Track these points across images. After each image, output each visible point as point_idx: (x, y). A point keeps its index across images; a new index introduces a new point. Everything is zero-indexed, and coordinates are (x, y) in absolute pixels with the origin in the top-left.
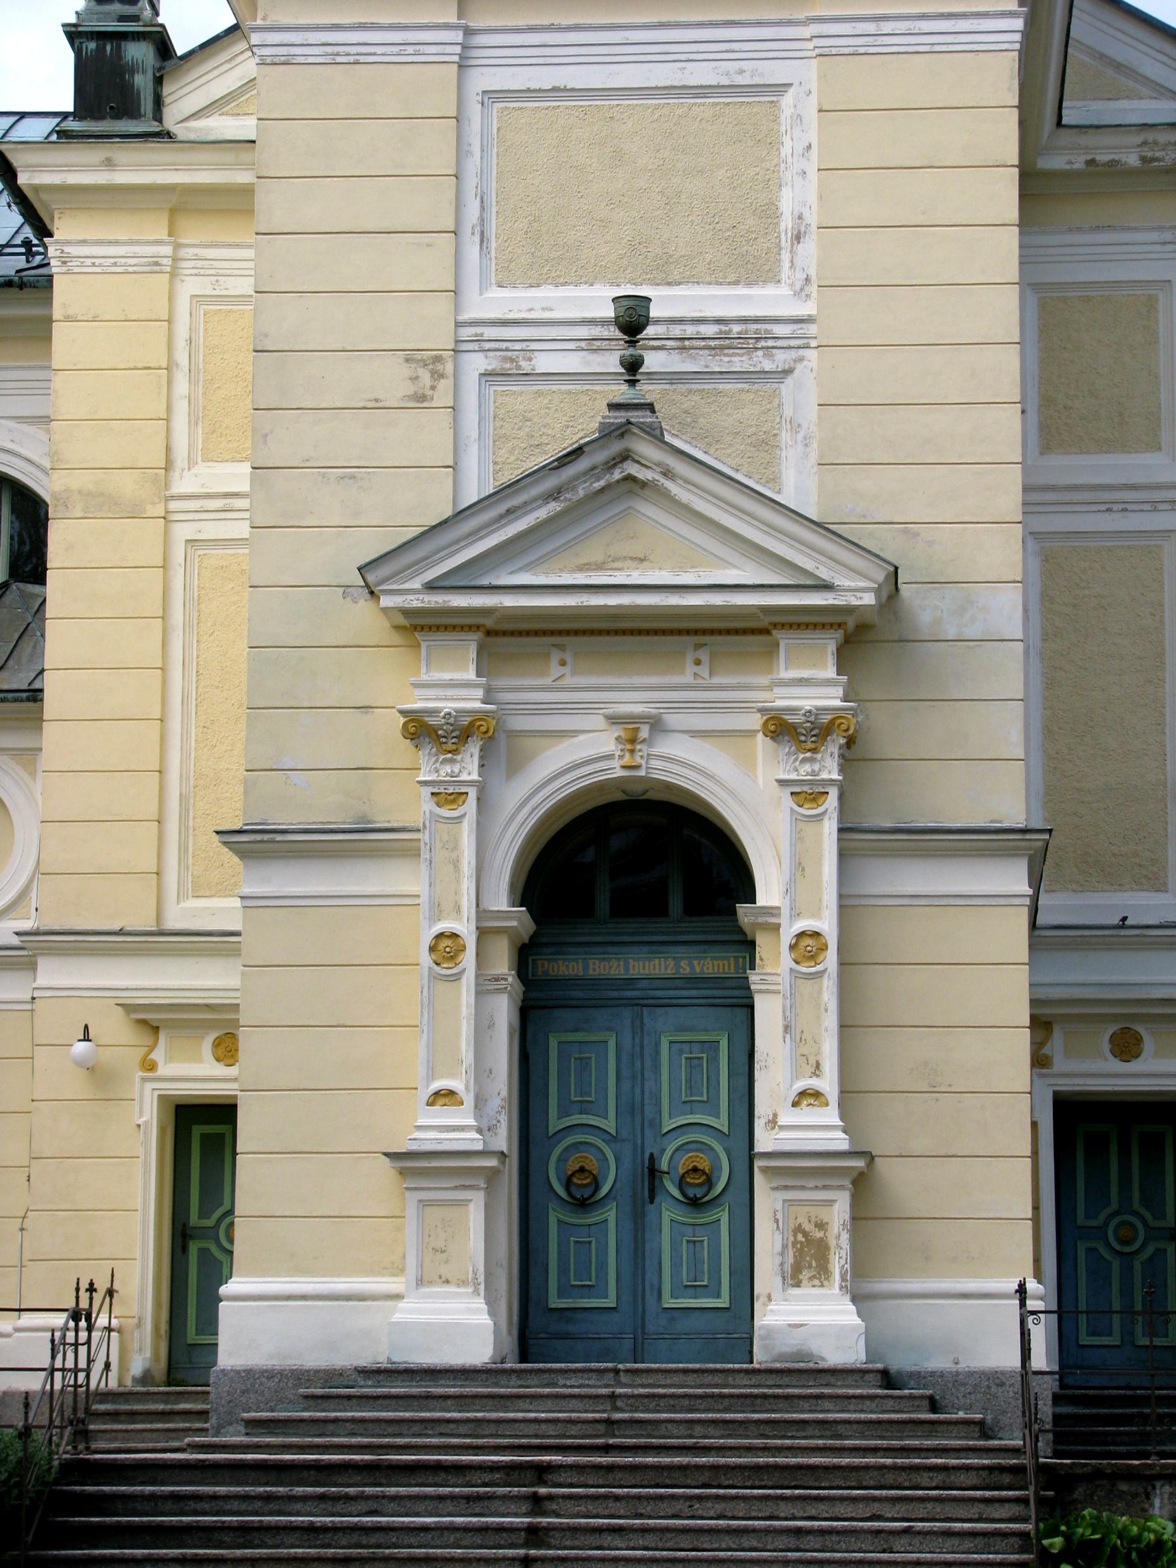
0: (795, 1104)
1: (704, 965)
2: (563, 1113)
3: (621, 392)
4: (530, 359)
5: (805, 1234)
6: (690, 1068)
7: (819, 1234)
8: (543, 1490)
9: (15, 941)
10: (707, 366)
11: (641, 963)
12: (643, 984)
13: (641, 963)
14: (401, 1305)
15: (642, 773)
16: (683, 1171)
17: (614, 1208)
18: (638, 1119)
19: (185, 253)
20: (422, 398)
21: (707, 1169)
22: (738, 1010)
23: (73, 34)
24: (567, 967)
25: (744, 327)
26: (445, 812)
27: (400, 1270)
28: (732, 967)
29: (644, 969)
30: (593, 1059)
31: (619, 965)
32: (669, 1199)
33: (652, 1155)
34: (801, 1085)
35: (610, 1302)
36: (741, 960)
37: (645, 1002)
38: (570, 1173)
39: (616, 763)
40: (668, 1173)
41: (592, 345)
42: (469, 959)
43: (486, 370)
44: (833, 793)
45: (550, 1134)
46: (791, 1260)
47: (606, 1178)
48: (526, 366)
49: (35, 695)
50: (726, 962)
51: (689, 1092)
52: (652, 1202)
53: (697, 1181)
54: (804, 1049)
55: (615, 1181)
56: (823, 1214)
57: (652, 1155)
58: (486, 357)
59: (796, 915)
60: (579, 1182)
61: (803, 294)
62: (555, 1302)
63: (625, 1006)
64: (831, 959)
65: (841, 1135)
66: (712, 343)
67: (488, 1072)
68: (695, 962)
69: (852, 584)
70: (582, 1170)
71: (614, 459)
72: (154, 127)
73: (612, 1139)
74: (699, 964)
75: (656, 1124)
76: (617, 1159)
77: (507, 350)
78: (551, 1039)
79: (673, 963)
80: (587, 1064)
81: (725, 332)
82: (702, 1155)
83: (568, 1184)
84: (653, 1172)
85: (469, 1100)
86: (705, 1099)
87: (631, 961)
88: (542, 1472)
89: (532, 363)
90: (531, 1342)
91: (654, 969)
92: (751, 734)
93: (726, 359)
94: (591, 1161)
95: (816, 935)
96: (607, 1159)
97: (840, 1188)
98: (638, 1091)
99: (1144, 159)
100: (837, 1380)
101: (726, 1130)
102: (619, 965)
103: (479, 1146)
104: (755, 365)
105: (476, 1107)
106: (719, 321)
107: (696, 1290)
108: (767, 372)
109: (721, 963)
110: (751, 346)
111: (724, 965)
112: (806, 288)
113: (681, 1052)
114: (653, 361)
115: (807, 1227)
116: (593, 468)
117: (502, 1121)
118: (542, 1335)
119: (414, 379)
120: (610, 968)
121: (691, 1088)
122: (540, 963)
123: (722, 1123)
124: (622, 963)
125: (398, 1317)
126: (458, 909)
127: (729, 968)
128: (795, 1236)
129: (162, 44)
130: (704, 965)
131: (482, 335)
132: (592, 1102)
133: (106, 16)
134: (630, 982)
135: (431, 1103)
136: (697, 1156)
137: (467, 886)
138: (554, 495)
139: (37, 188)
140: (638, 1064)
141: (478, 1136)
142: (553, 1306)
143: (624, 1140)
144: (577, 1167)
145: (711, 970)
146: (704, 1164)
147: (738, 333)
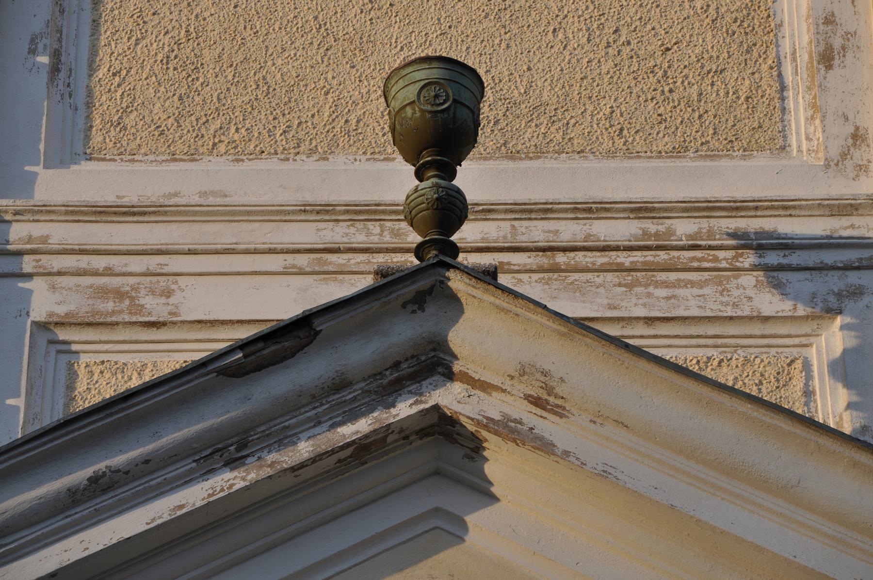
4: (168, 293)
10: (613, 307)
25: (704, 224)
43: (51, 315)
58: (53, 288)
61: (849, 164)
71: (396, 365)
77: (109, 272)
81: (657, 235)
89: (172, 300)
93: (662, 292)
108: (766, 319)
110: (724, 265)
112: (856, 154)
116: (340, 384)
131: (45, 239)
147: (690, 237)
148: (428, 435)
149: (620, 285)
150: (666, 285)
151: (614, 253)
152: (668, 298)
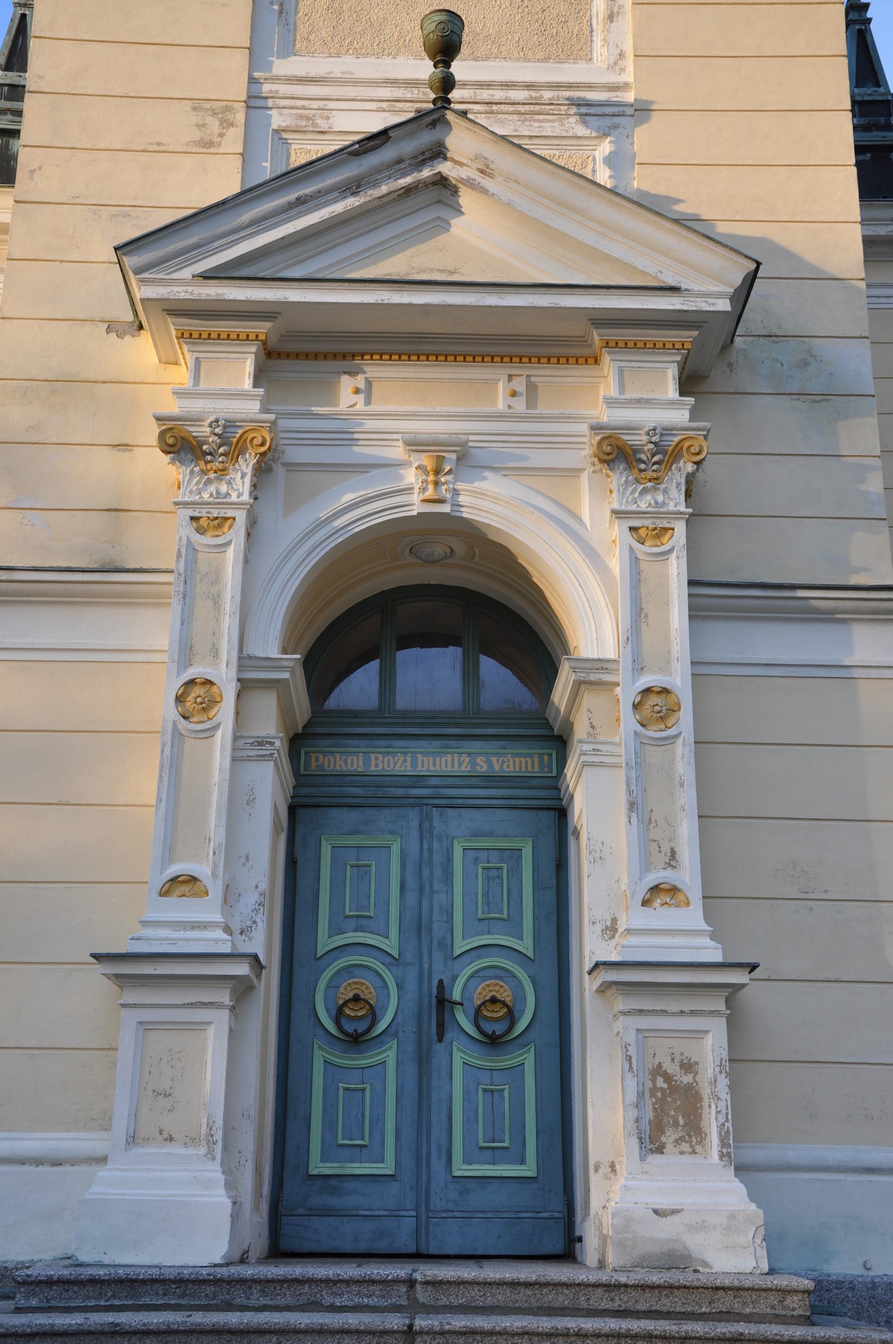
0: (645, 903)
1: (503, 762)
2: (336, 930)
4: (328, 118)
5: (668, 1078)
6: (488, 879)
7: (687, 1079)
10: (516, 131)
11: (431, 759)
12: (433, 781)
13: (431, 759)
14: (103, 1173)
15: (446, 508)
16: (479, 1003)
17: (395, 1046)
18: (425, 939)
20: (210, 144)
21: (508, 1000)
22: (543, 814)
24: (345, 762)
25: (556, 93)
26: (207, 540)
27: (105, 1123)
28: (536, 765)
29: (434, 765)
30: (373, 866)
31: (405, 761)
32: (463, 1038)
33: (441, 982)
34: (654, 878)
35: (387, 1168)
36: (546, 758)
37: (437, 802)
38: (341, 1002)
39: (416, 498)
40: (461, 1004)
42: (226, 711)
43: (280, 126)
44: (680, 528)
45: (319, 955)
46: (650, 1114)
47: (385, 1008)
48: (323, 125)
50: (529, 760)
51: (486, 908)
52: (440, 1040)
53: (496, 1015)
54: (654, 833)
55: (396, 1014)
56: (690, 1050)
57: (441, 982)
58: (280, 114)
59: (639, 668)
60: (352, 1014)
61: (617, 67)
62: (317, 1167)
63: (413, 806)
64: (685, 720)
65: (707, 941)
66: (522, 108)
67: (243, 860)
68: (494, 759)
69: (704, 288)
70: (356, 999)
71: (423, 153)
73: (394, 962)
74: (498, 761)
75: (446, 945)
76: (399, 987)
77: (303, 108)
78: (324, 843)
79: (467, 759)
80: (365, 873)
81: (536, 98)
82: (501, 984)
83: (338, 1016)
84: (443, 1003)
85: (216, 890)
86: (505, 916)
87: (419, 756)
89: (330, 121)
90: (284, 1220)
91: (446, 766)
92: (575, 472)
93: (536, 124)
94: (367, 988)
95: (665, 691)
96: (387, 986)
97: (713, 1013)
98: (425, 904)
100: (745, 1304)
101: (530, 954)
102: (405, 761)
103: (226, 949)
104: (567, 131)
105: (225, 901)
106: (530, 86)
107: (495, 1154)
108: (579, 138)
109: (523, 760)
110: (563, 112)
111: (526, 762)
112: (620, 63)
113: (476, 860)
115: (671, 1068)
116: (400, 161)
117: (258, 920)
118: (301, 1211)
119: (202, 126)
120: (395, 764)
121: (488, 904)
122: (313, 756)
123: (526, 946)
124: (409, 759)
125: (96, 1190)
126: (215, 652)
127: (533, 767)
128: (654, 1081)
130: (503, 762)
131: (277, 92)
132: (370, 917)
134: (418, 780)
135: (164, 893)
136: (497, 984)
137: (229, 624)
138: (353, 187)
140: (426, 873)
141: (225, 936)
142: (313, 1171)
143: (408, 964)
144: (351, 995)
145: (511, 769)
146: (505, 995)
147: (549, 99)
148: (436, 185)
149: (519, 121)
150: (538, 121)
151: (517, 106)
152: (539, 127)
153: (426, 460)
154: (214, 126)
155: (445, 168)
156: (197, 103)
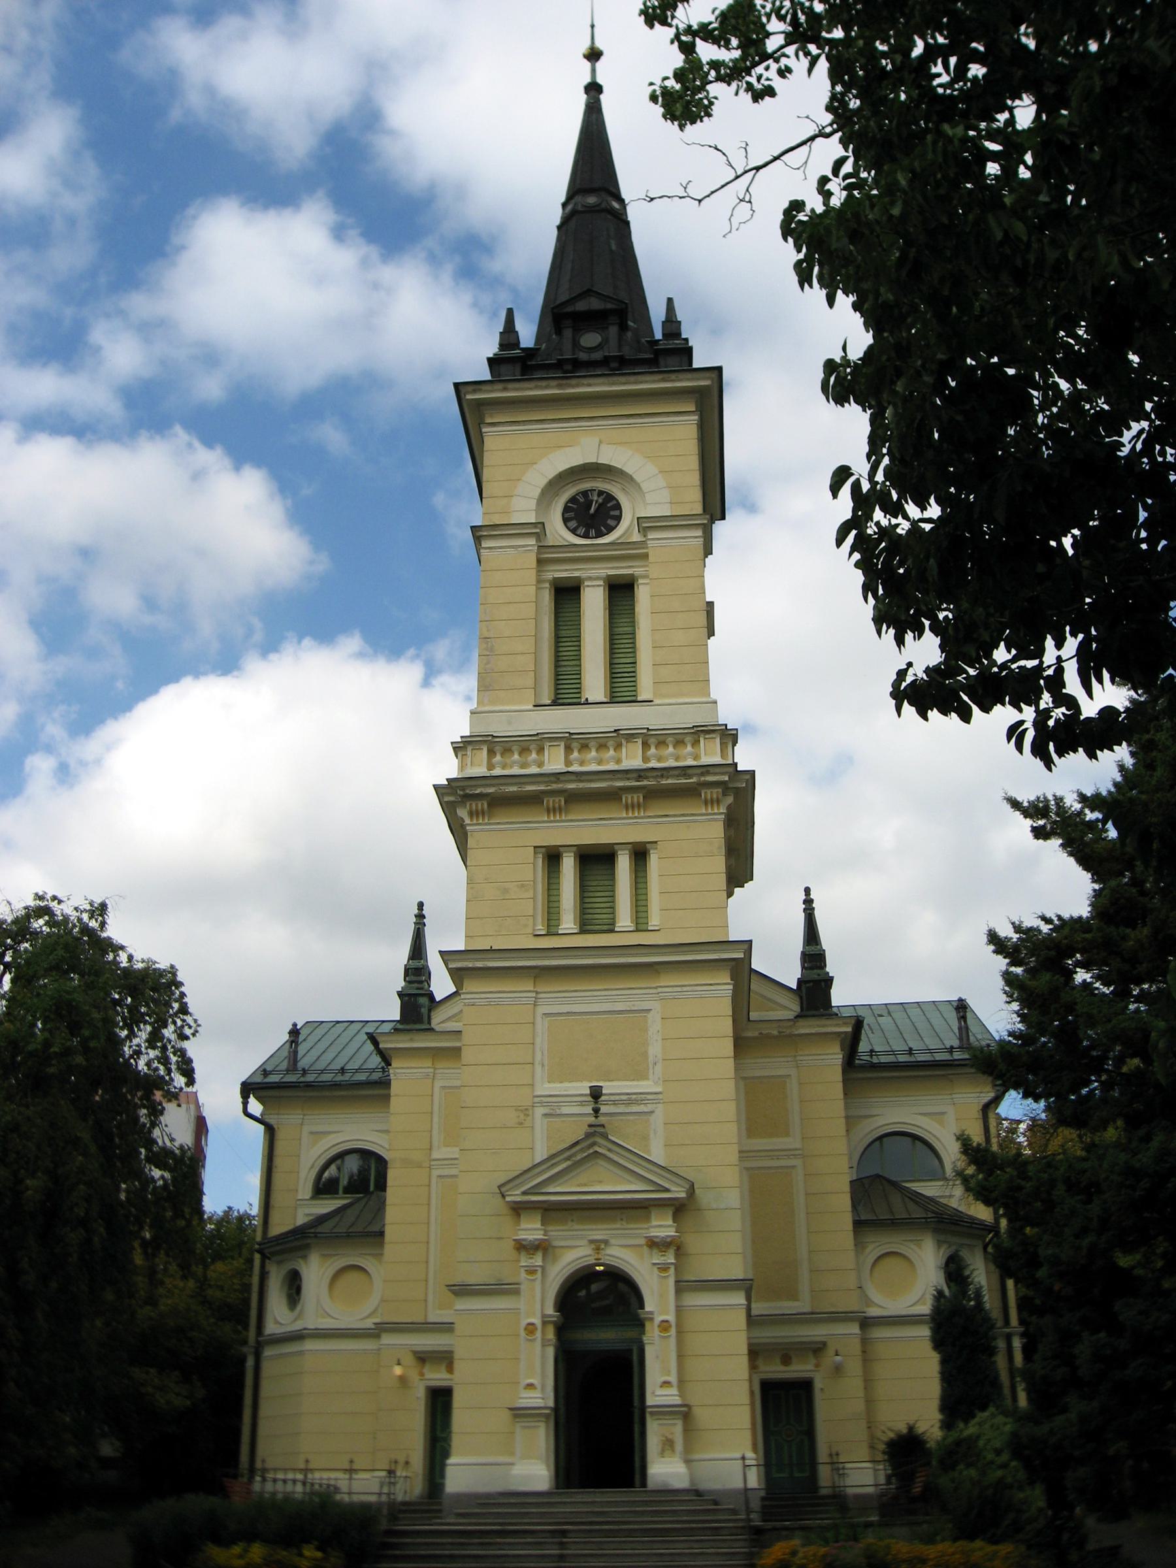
3: (592, 1120)
8: (565, 1540)
9: (373, 1327)
19: (437, 1071)
23: (400, 994)
41: (582, 1104)
42: (539, 1334)
48: (558, 1112)
49: (381, 1234)
64: (673, 1331)
69: (677, 1189)
72: (427, 1027)
85: (539, 1386)
88: (564, 1533)
97: (679, 1419)
99: (779, 1032)
103: (542, 1405)
114: (604, 1109)
116: (583, 1148)
129: (431, 996)
133: (411, 988)
137: (538, 1306)
138: (568, 1159)
139: (386, 1049)
153: (593, 1246)
154: (522, 1116)
155: (597, 1149)
156: (517, 1109)
